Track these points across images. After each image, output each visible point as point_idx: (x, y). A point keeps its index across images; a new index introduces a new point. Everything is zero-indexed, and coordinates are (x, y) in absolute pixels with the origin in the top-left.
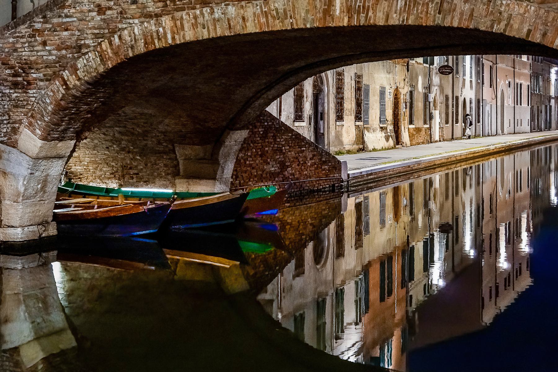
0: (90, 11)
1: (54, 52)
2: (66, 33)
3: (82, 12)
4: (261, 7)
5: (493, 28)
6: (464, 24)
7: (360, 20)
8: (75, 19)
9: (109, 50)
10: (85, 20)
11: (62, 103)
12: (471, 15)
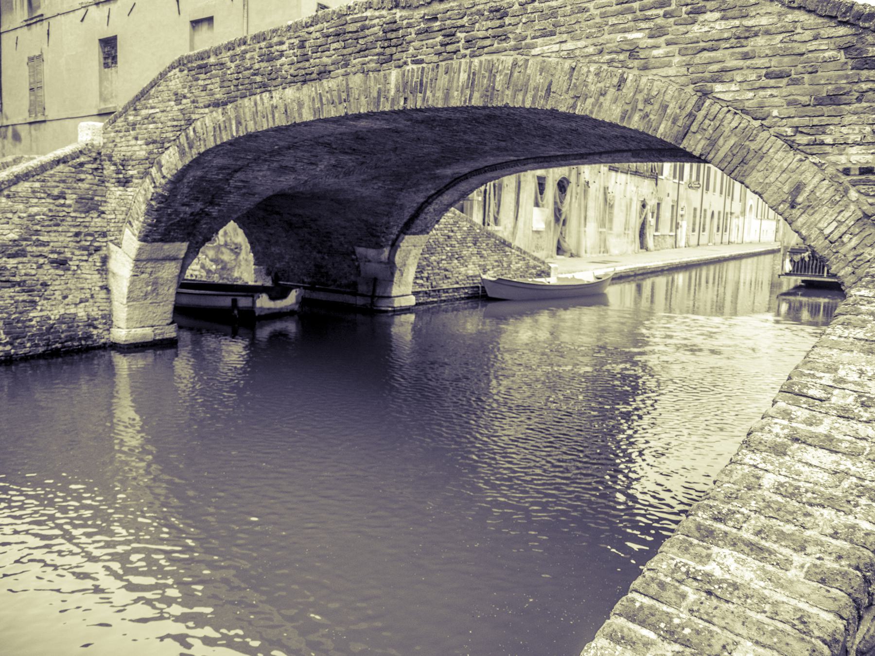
0: (169, 100)
2: (151, 126)
5: (575, 109)
6: (540, 104)
11: (153, 203)
12: (549, 90)
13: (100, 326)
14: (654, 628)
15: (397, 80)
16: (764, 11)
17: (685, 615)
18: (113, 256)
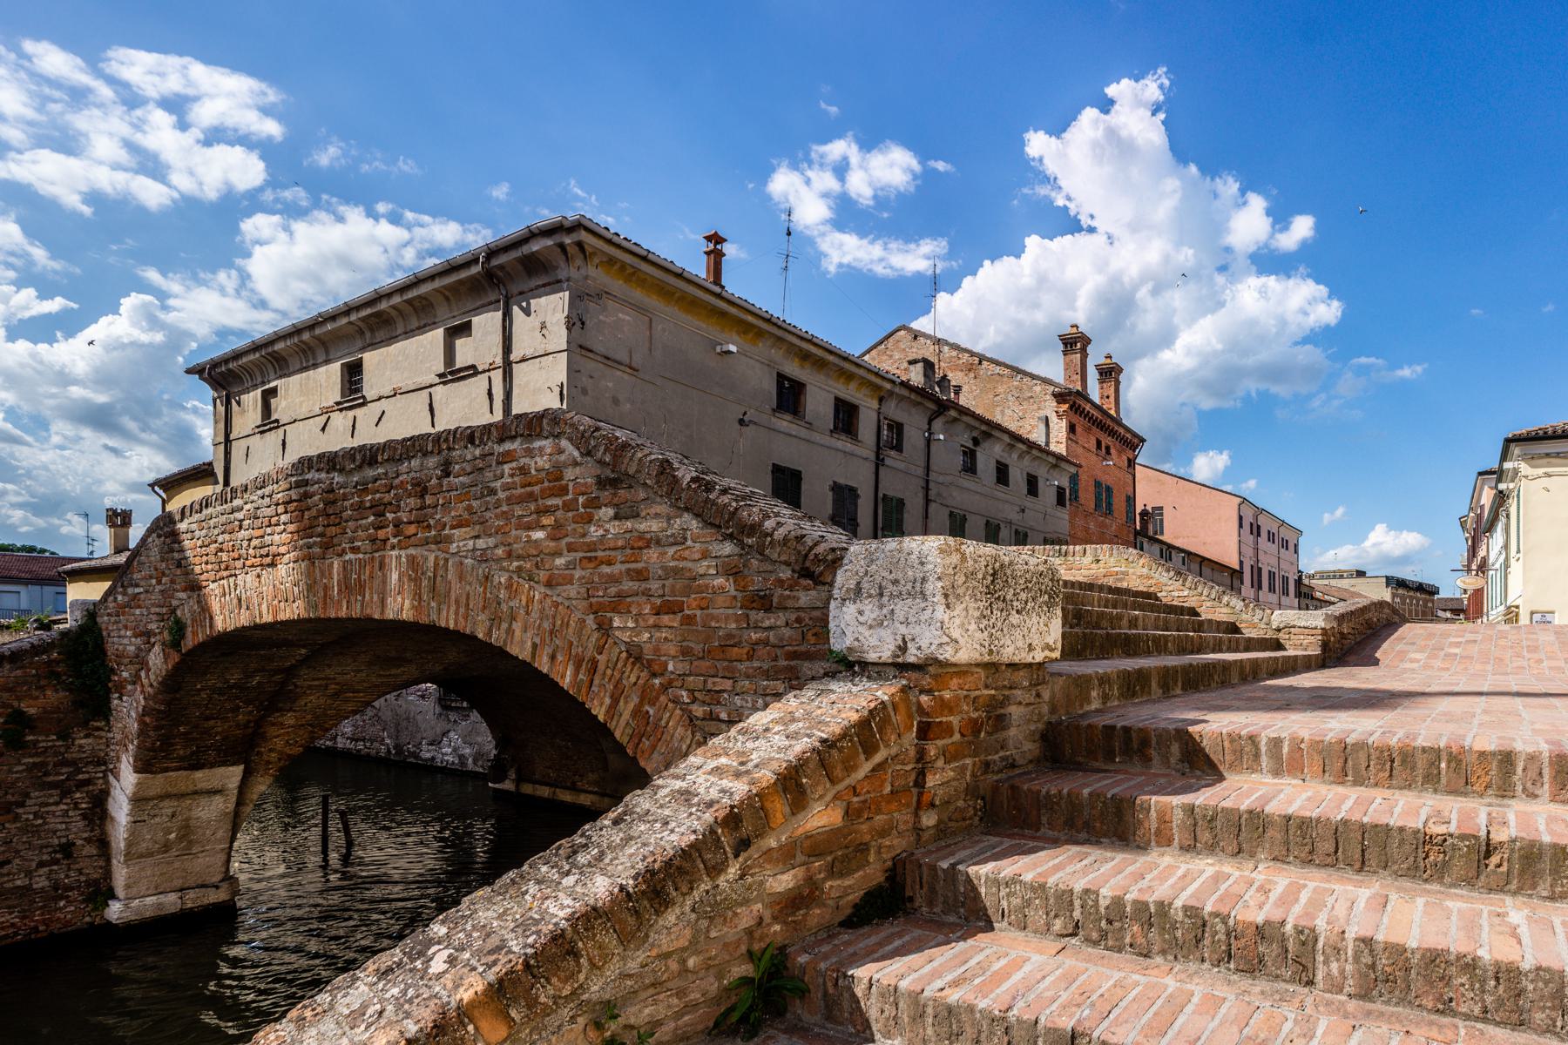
16: (652, 511)
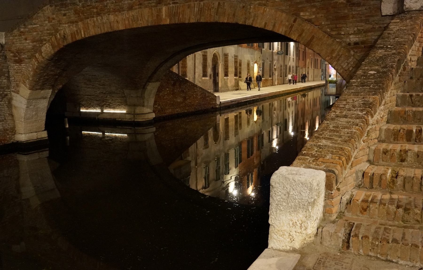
0: (45, 21)
1: (31, 44)
2: (35, 33)
3: (41, 21)
4: (125, 15)
5: (246, 23)
7: (176, 21)
8: (38, 25)
9: (55, 42)
10: (43, 26)
12: (234, 15)
13: (10, 133)
14: (308, 156)
15: (166, 11)
17: (315, 153)
18: (14, 98)
